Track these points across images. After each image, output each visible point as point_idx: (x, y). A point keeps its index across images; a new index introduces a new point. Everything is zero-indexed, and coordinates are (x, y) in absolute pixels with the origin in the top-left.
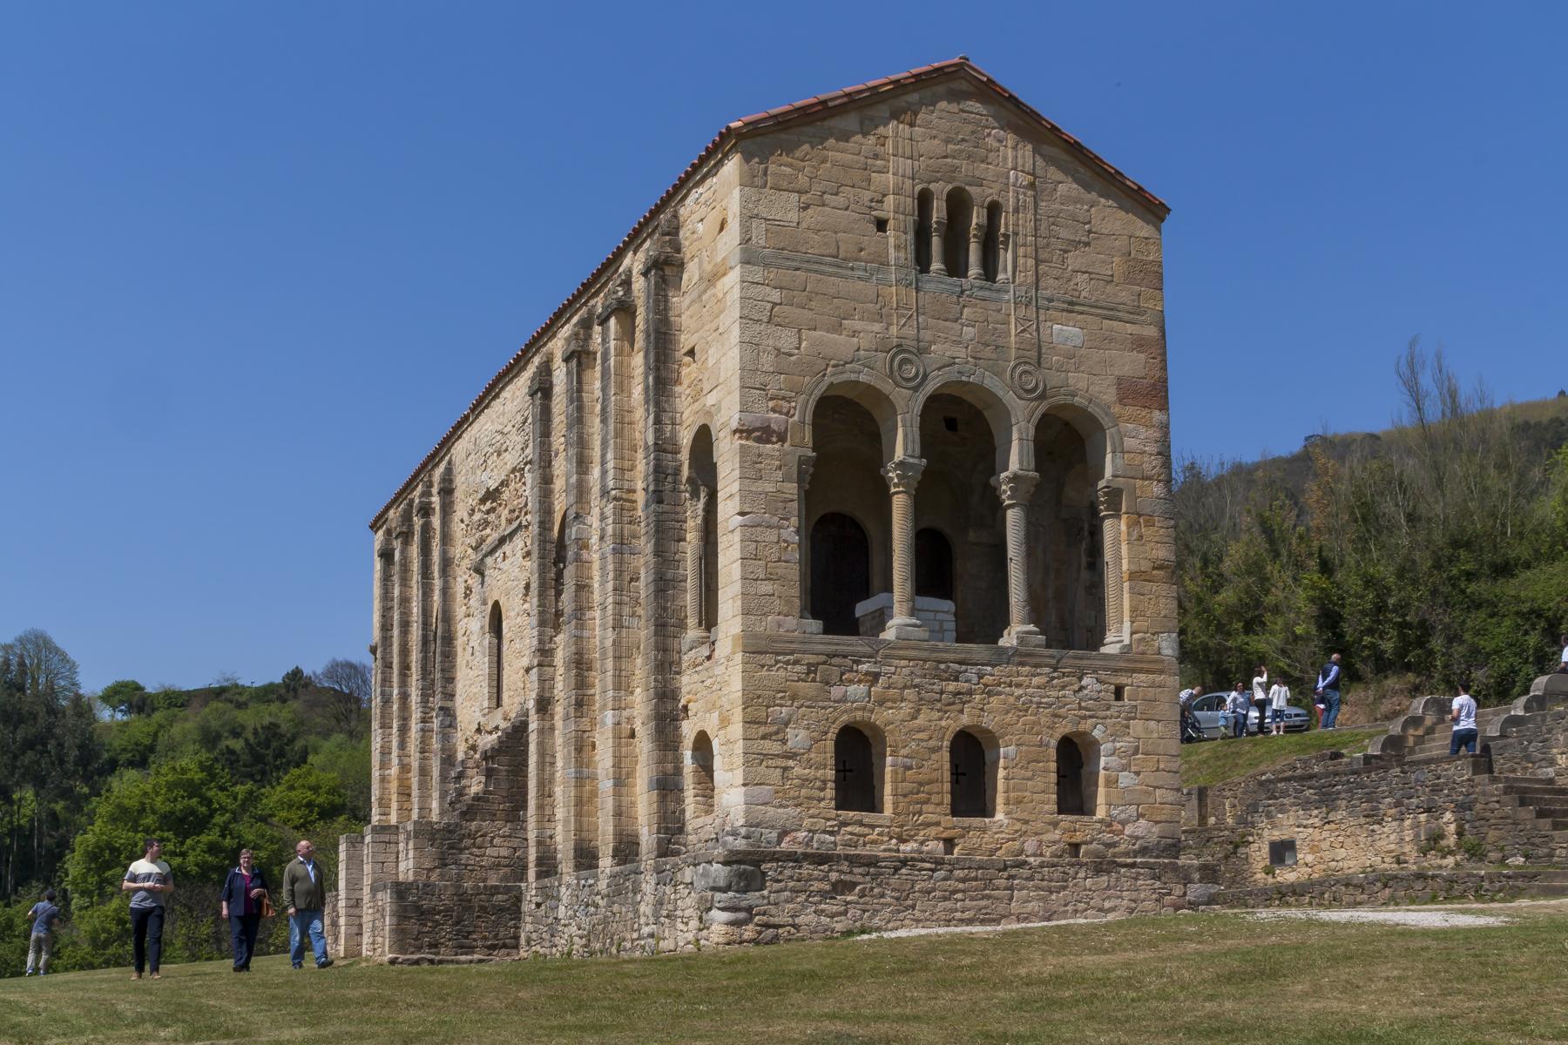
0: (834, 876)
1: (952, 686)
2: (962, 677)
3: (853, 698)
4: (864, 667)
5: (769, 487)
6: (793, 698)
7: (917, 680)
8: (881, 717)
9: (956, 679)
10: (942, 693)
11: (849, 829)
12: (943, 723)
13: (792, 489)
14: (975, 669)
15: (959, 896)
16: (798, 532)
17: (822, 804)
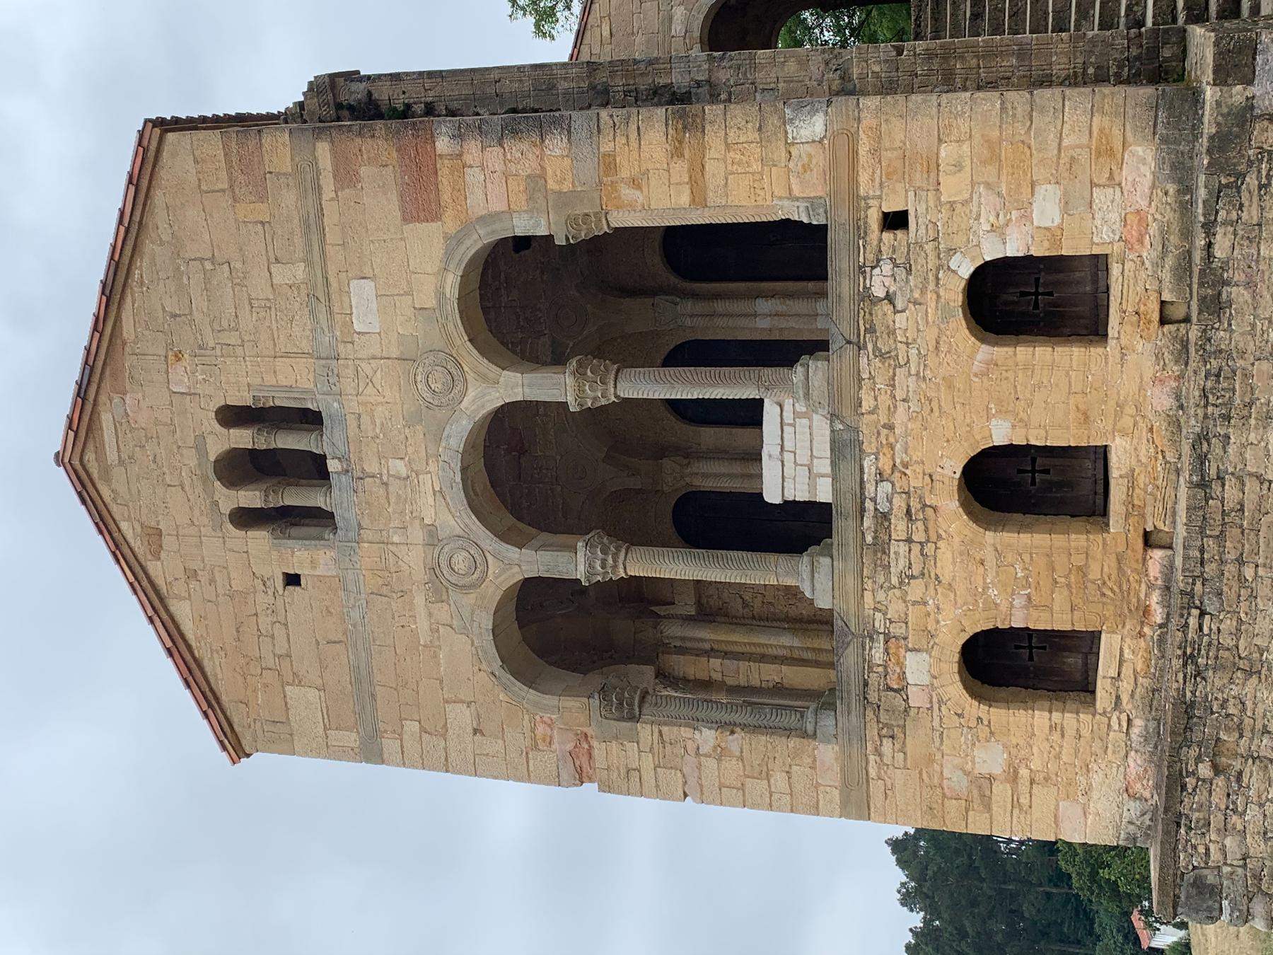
0: (1205, 770)
1: (899, 527)
2: (883, 507)
3: (930, 671)
4: (878, 655)
5: (648, 762)
6: (930, 760)
7: (895, 580)
8: (952, 643)
9: (885, 516)
10: (909, 540)
11: (1125, 698)
12: (957, 540)
13: (645, 731)
14: (870, 489)
15: (1249, 572)
16: (695, 723)
17: (1085, 732)
